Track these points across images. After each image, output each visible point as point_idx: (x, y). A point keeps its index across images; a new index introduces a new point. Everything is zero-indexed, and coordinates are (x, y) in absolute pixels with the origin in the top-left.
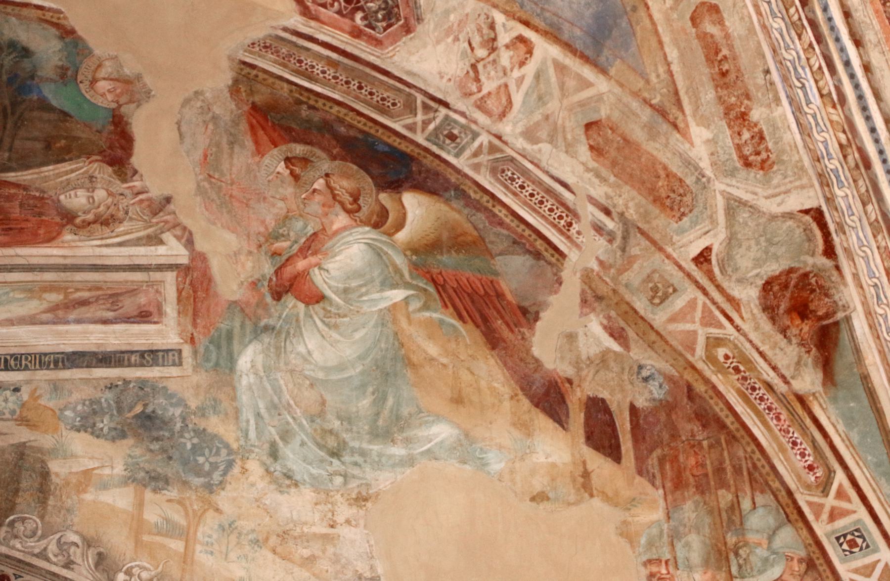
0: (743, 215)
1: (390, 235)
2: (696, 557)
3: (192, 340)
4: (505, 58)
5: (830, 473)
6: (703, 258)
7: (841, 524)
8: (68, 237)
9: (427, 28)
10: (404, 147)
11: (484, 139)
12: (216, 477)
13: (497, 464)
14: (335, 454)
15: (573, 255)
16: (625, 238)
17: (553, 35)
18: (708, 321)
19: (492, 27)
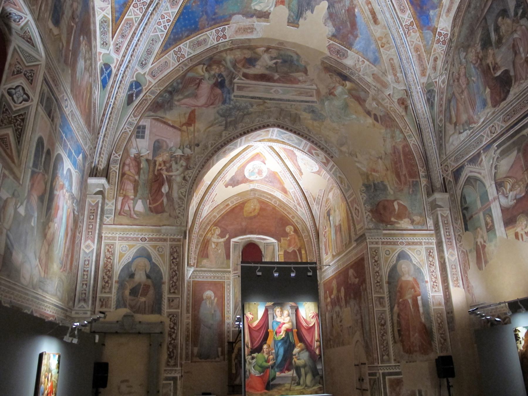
0: (395, 89)
1: (345, 87)
2: (389, 137)
3: (318, 100)
4: (360, 63)
5: (407, 127)
6: (389, 95)
7: (408, 134)
8: (300, 83)
9: (349, 57)
10: (346, 75)
11: (357, 75)
12: (323, 120)
13: (362, 122)
14: (340, 118)
15: (370, 93)
16: (378, 91)
17: (368, 60)
18: (390, 104)
19: (359, 58)
